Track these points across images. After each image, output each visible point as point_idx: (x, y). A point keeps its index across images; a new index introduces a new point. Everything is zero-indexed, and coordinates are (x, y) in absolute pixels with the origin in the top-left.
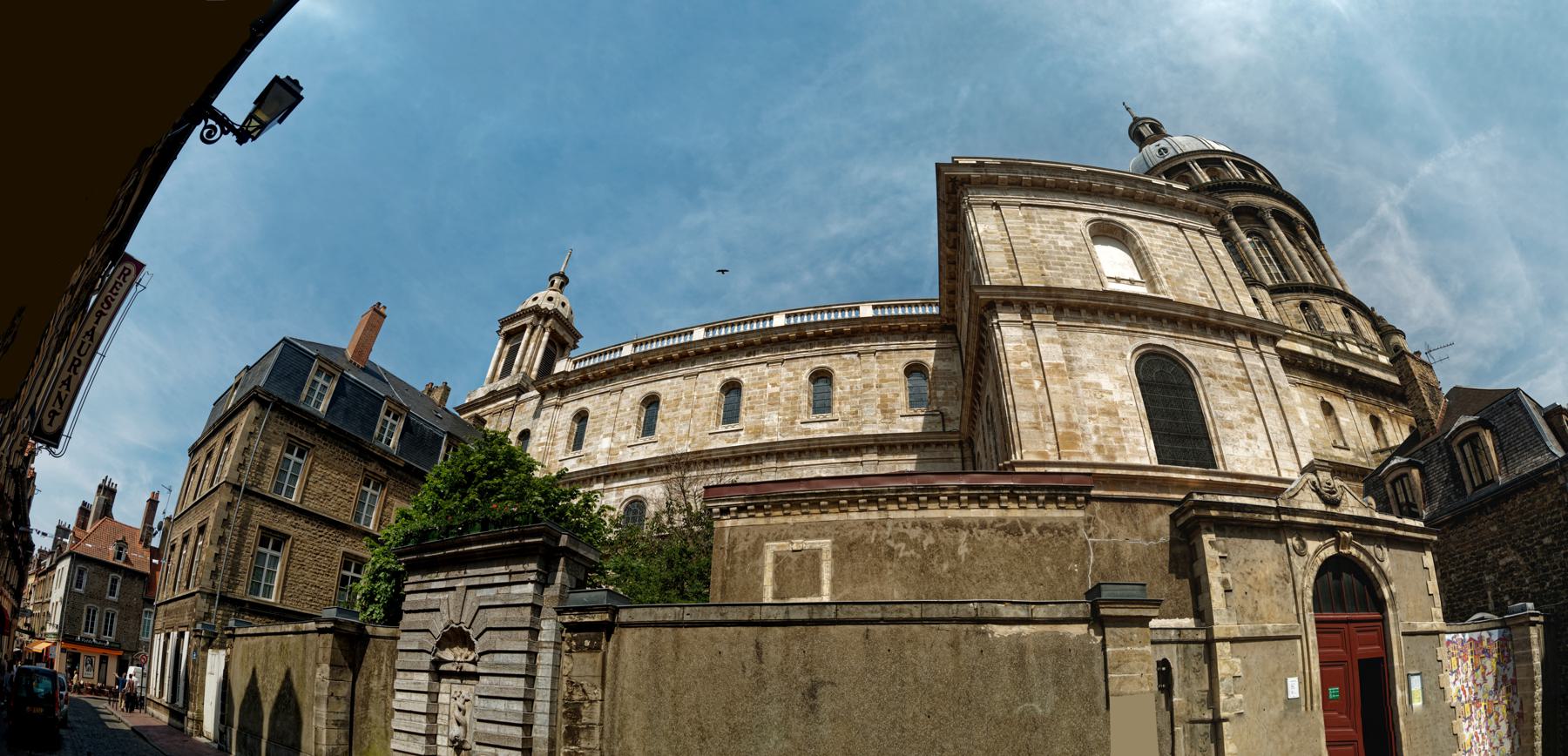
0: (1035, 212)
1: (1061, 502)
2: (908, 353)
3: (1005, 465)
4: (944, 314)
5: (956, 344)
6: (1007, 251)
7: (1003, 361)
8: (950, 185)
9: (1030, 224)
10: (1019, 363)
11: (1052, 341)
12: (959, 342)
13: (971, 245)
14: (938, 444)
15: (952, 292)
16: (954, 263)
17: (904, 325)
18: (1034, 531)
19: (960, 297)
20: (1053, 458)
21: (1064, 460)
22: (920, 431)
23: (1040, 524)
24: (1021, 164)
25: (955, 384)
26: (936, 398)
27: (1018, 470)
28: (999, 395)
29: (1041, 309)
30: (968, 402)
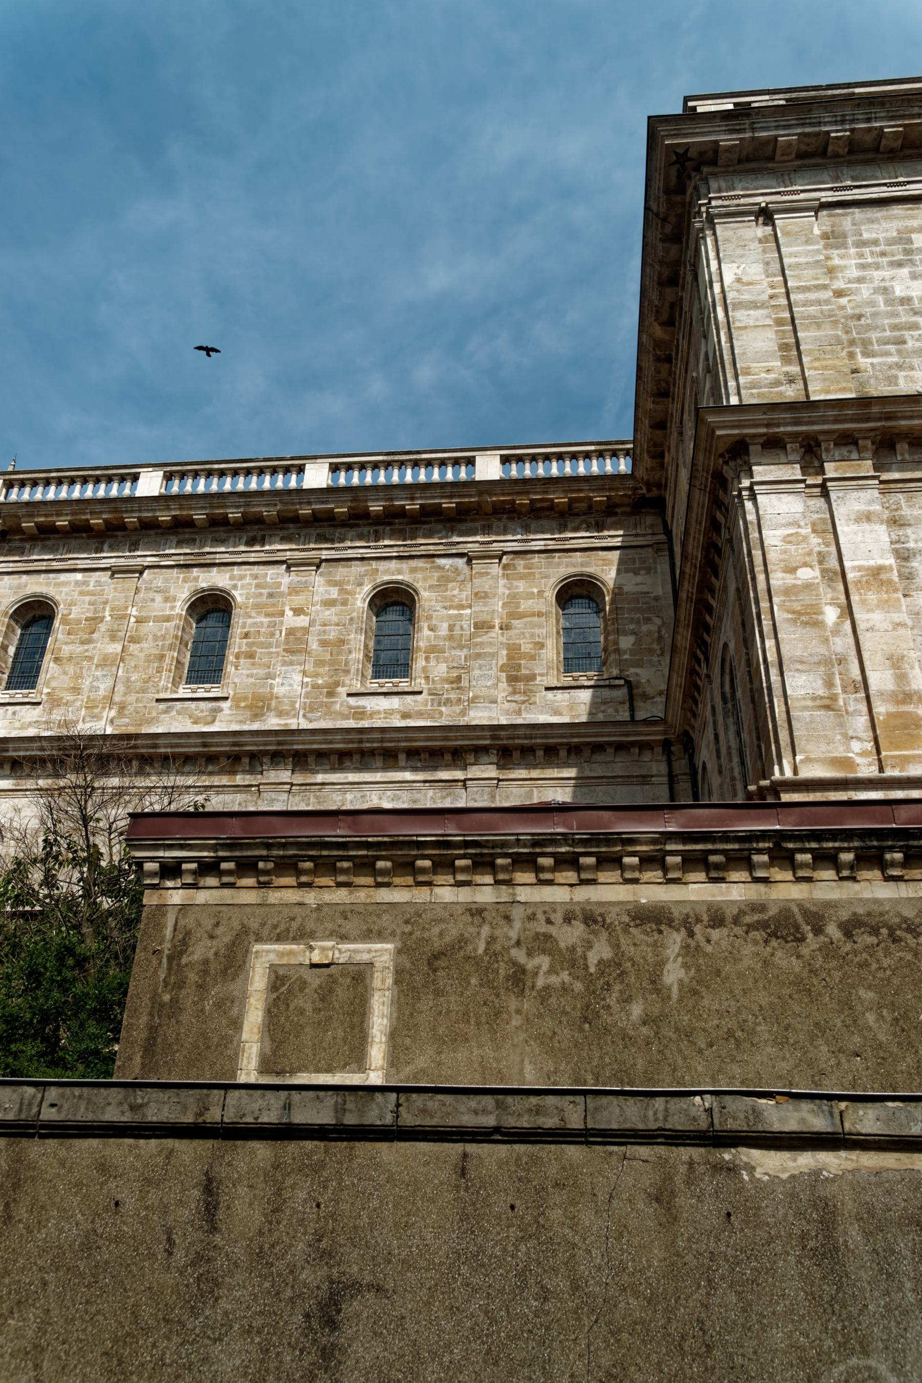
0: (848, 220)
1: (893, 864)
2: (566, 559)
3: (760, 788)
4: (641, 473)
5: (663, 537)
6: (779, 322)
7: (759, 568)
8: (673, 171)
9: (835, 252)
10: (792, 570)
11: (868, 517)
12: (668, 532)
13: (705, 315)
14: (620, 747)
15: (660, 425)
16: (669, 359)
17: (560, 499)
18: (832, 930)
19: (675, 435)
20: (867, 769)
21: (890, 773)
22: (584, 719)
23: (844, 915)
24: (833, 100)
25: (658, 621)
26: (618, 651)
27: (786, 797)
28: (747, 642)
29: (844, 451)
30: (683, 659)
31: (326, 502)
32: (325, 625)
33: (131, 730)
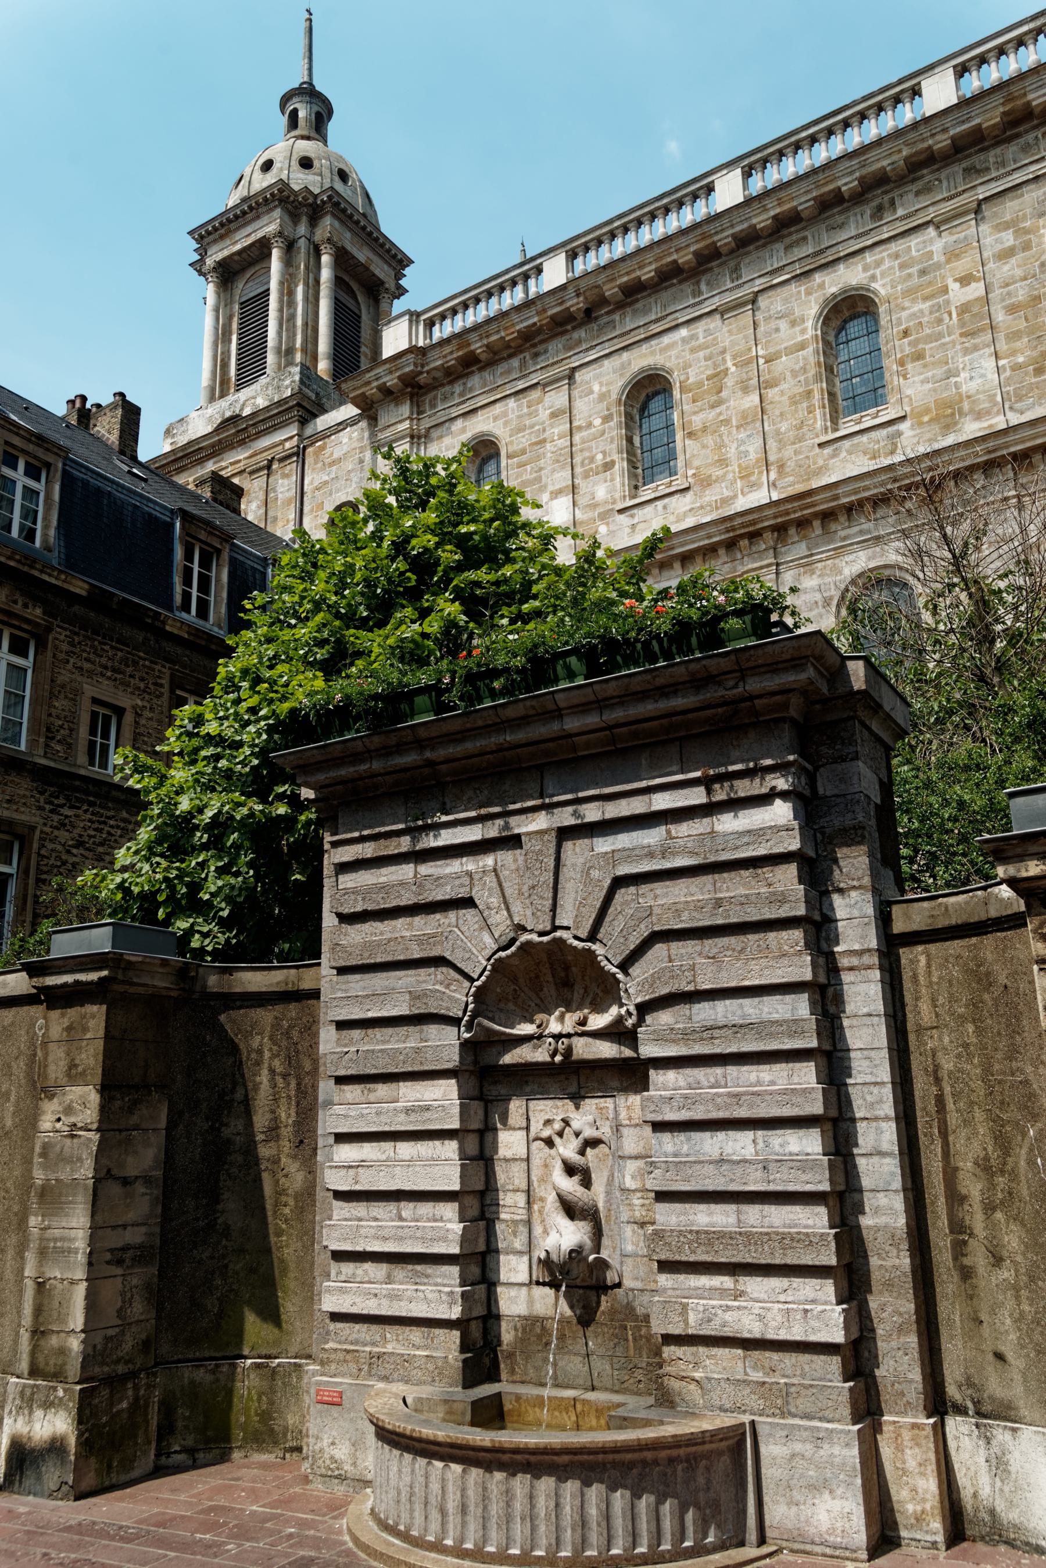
31: (968, 120)
32: (1007, 285)
33: (800, 488)
